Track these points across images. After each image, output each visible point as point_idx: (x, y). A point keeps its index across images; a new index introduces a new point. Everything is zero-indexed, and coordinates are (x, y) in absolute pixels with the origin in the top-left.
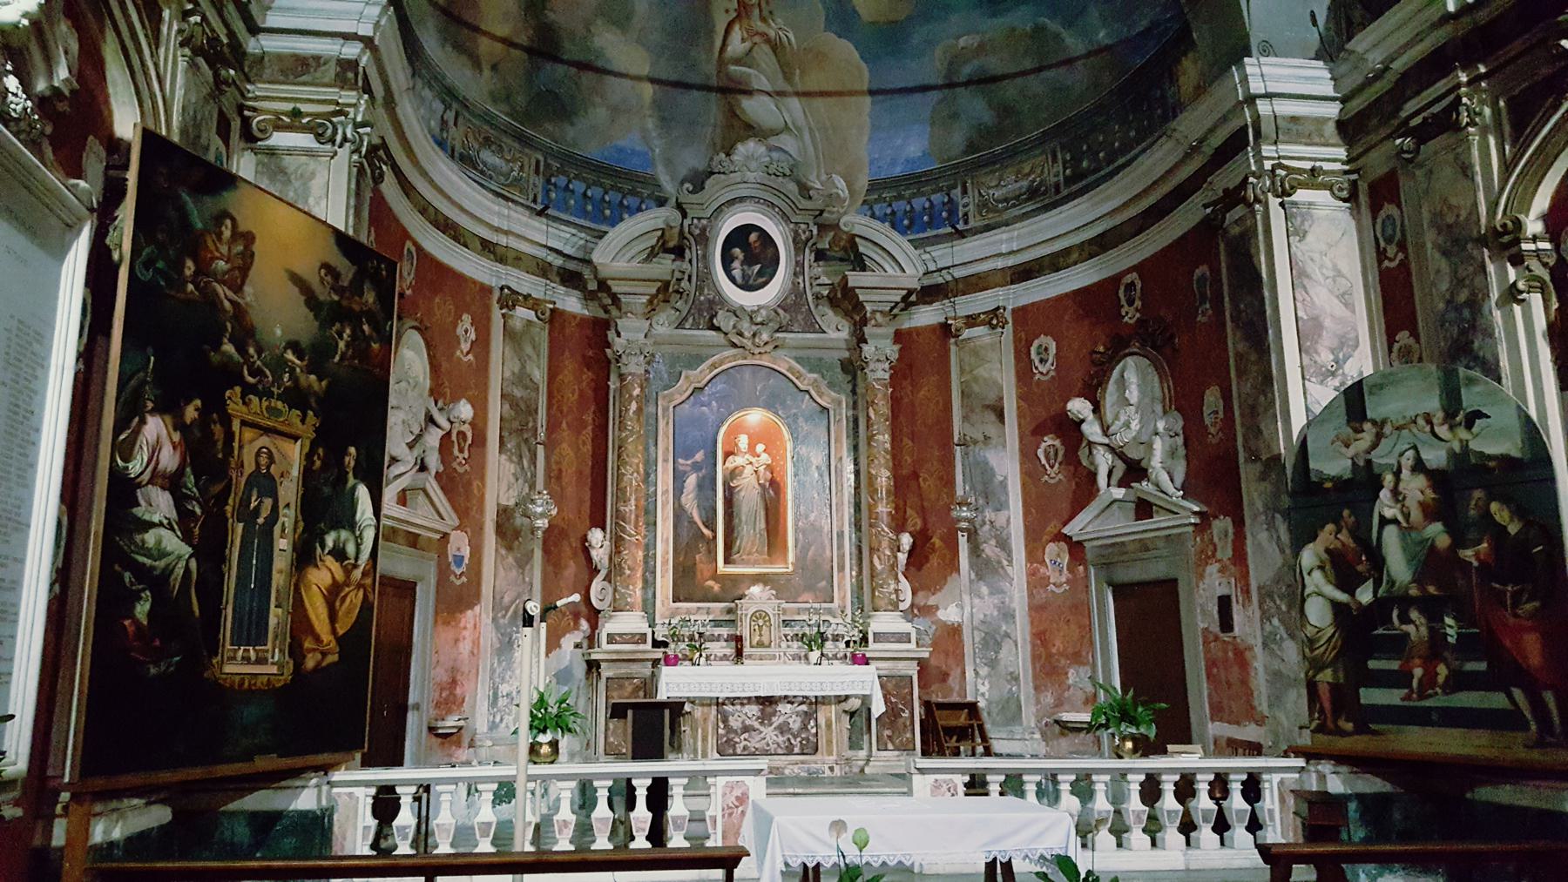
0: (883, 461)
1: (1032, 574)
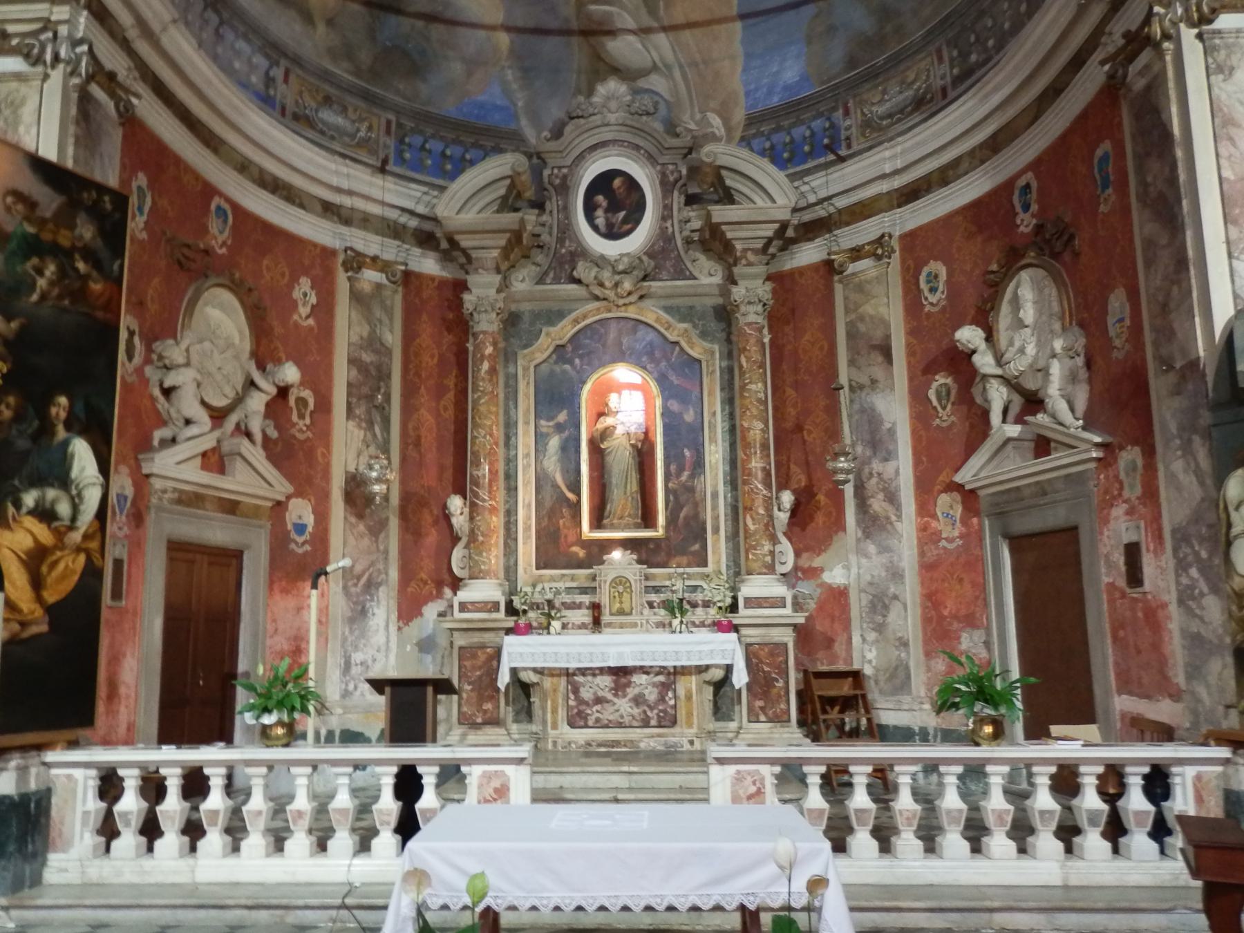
0: (755, 411)
1: (923, 529)
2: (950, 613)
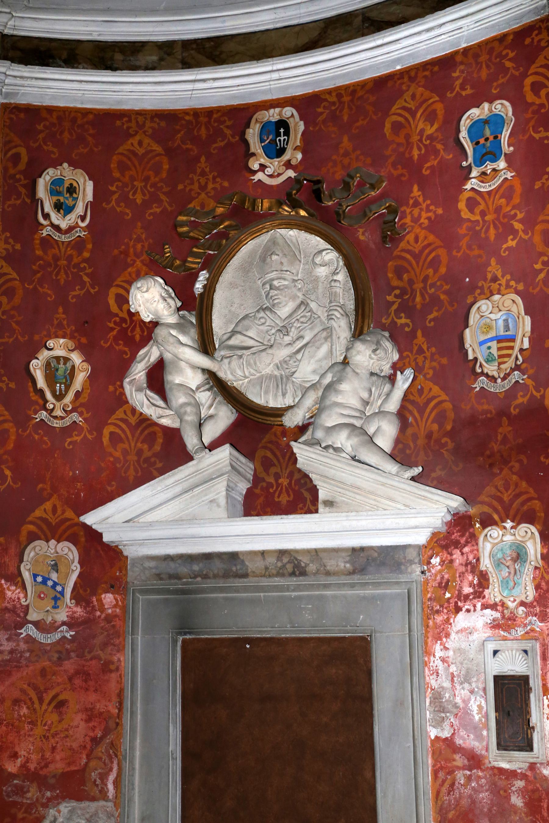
2: (24, 766)
